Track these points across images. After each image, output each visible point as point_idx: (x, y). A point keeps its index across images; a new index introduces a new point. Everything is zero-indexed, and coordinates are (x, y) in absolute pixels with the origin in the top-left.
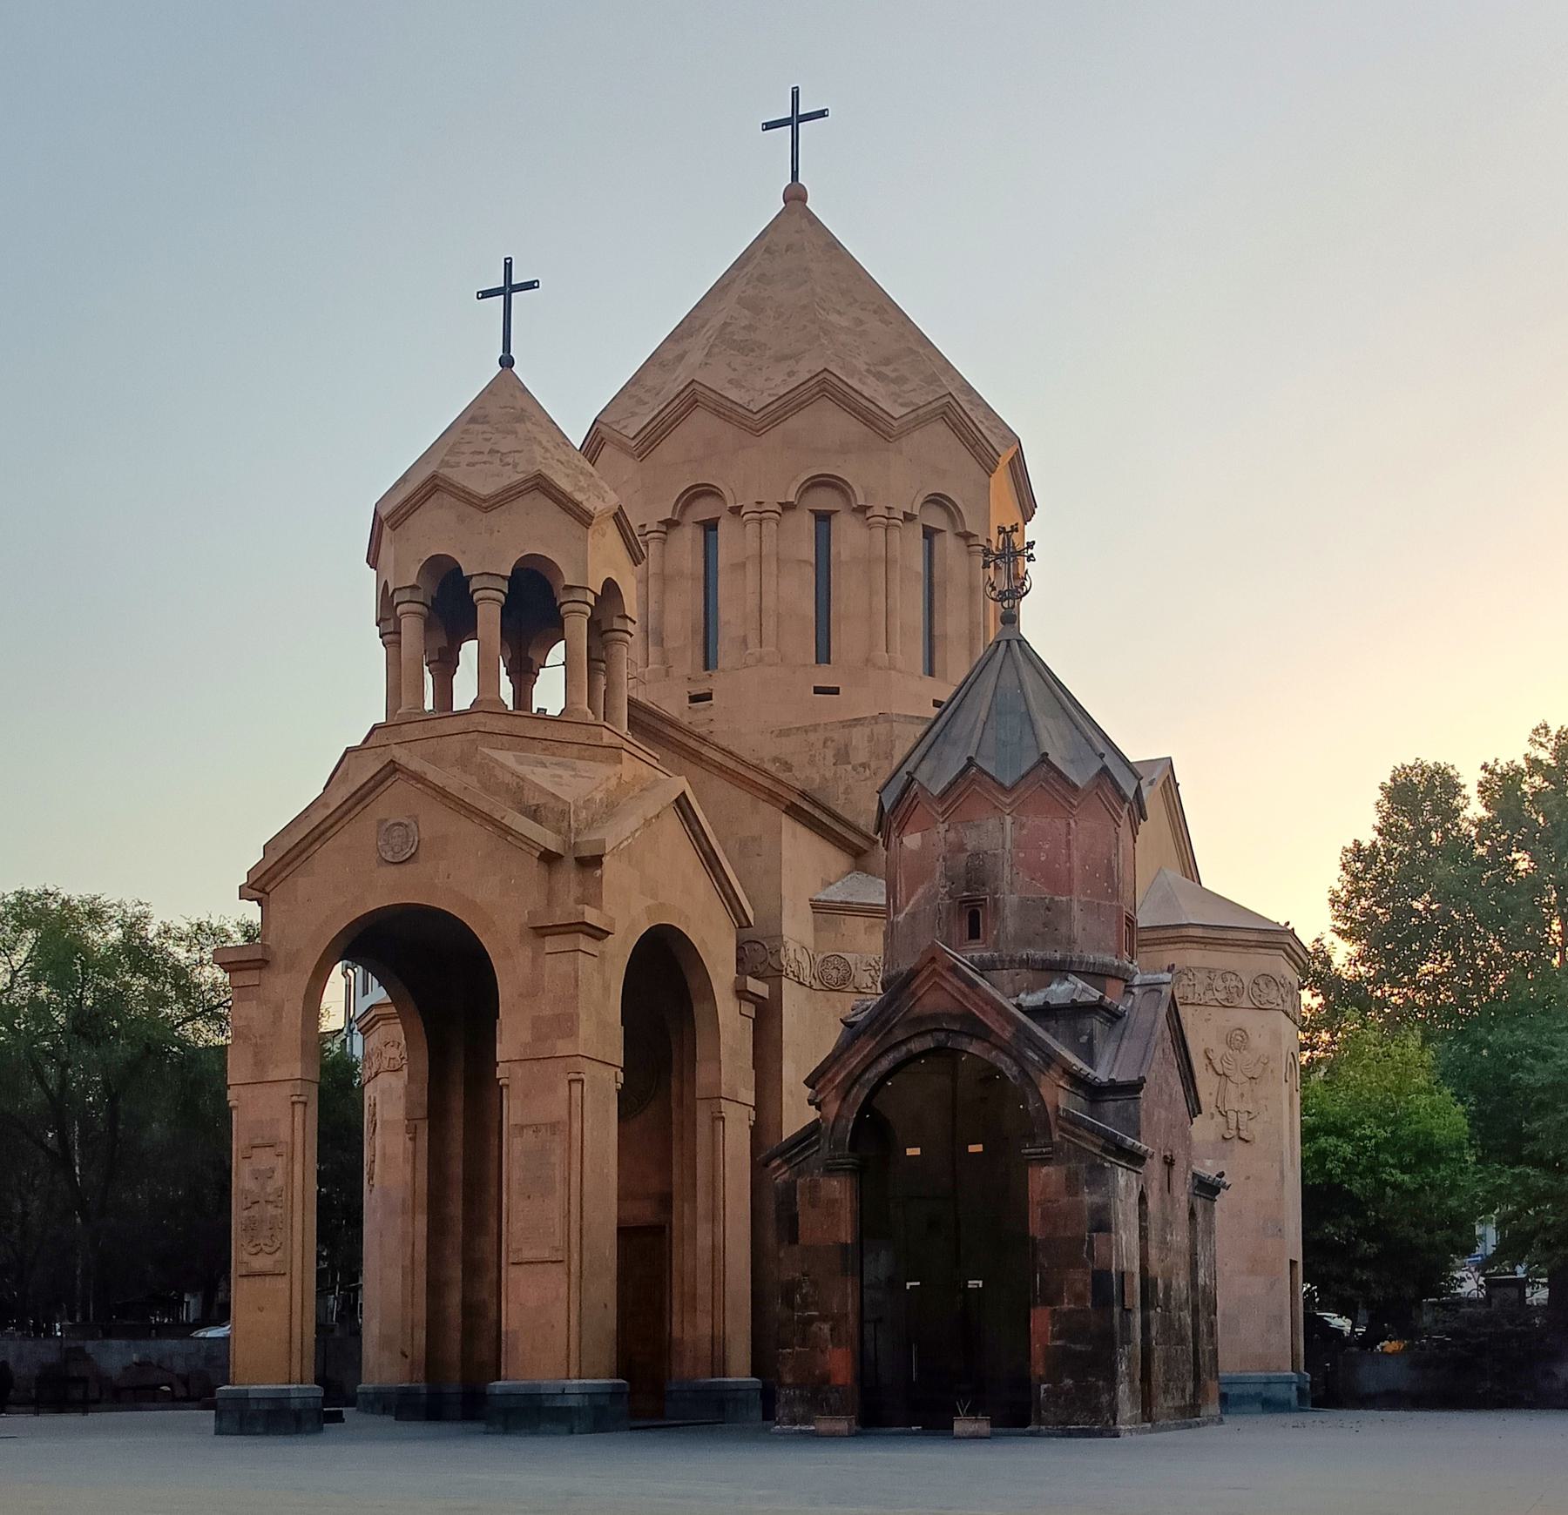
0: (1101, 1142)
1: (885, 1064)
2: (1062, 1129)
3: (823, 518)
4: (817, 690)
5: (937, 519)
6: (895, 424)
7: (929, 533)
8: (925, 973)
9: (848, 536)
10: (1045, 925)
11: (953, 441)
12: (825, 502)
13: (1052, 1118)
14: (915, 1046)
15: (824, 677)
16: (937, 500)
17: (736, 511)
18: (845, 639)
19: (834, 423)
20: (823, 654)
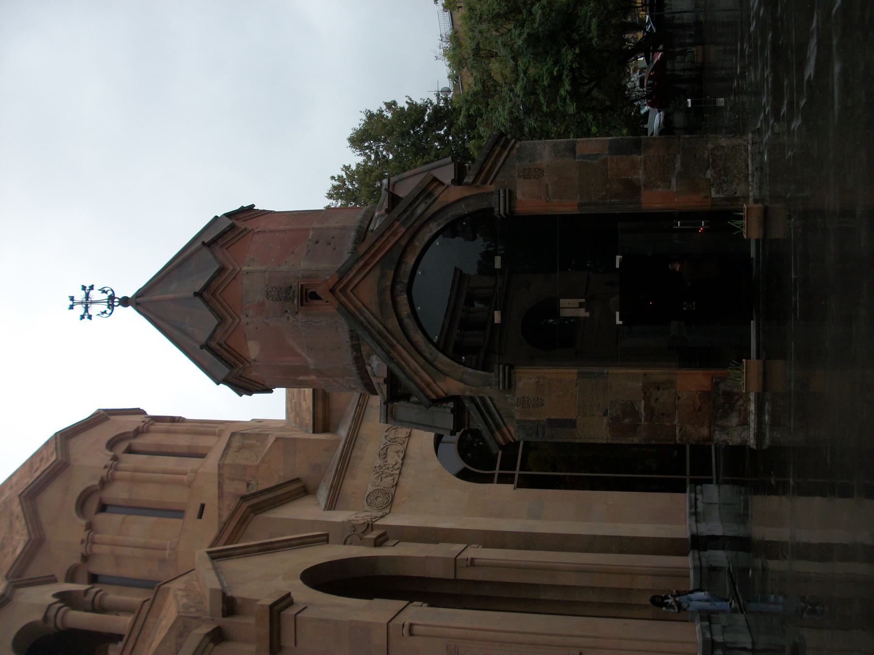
0: (498, 149)
1: (418, 337)
2: (484, 182)
3: (103, 508)
4: (200, 516)
5: (124, 446)
6: (60, 459)
7: (130, 451)
8: (343, 298)
9: (117, 493)
10: (329, 244)
11: (82, 436)
12: (94, 503)
13: (475, 191)
14: (405, 310)
15: (192, 512)
16: (112, 445)
17: (85, 558)
18: (174, 496)
19: (52, 495)
20: (178, 513)
